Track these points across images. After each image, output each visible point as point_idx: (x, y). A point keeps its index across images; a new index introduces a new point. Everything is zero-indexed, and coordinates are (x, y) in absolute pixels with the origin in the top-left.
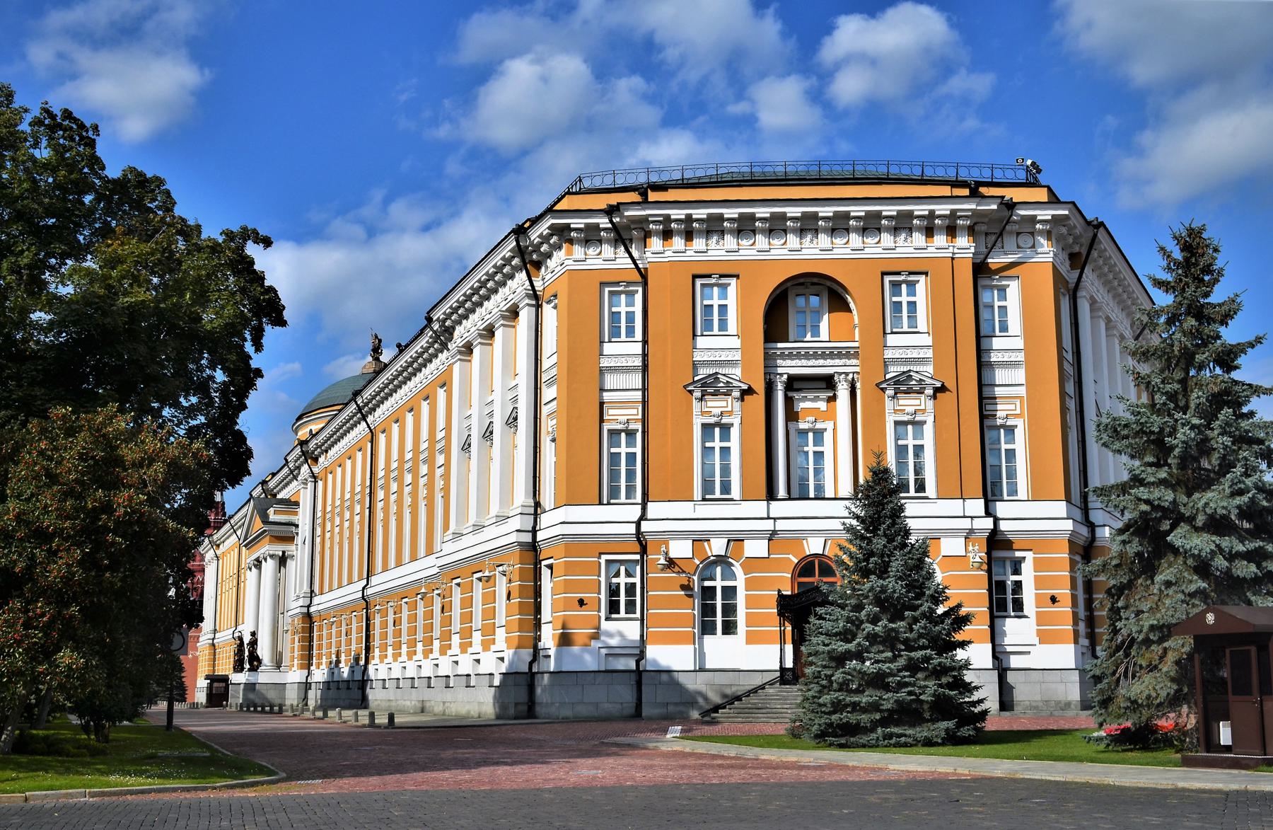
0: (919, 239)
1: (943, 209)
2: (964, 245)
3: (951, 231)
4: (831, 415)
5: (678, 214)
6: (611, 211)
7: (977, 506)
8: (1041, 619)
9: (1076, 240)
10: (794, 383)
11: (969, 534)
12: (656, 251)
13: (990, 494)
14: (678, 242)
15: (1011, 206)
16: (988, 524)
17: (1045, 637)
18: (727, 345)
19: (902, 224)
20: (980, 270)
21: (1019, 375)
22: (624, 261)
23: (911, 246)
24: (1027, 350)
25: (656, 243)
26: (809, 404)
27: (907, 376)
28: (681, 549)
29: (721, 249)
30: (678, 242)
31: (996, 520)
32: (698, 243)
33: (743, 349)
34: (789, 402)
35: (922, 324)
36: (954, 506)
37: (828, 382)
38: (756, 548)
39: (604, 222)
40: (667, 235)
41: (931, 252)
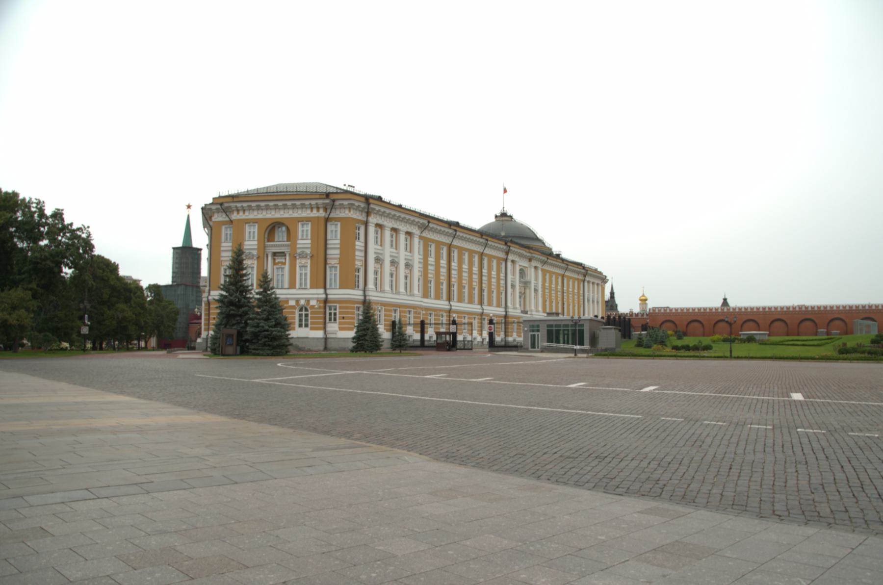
0: (309, 211)
1: (313, 202)
2: (322, 213)
3: (318, 209)
4: (284, 264)
5: (239, 205)
6: (221, 204)
7: (322, 291)
8: (340, 323)
9: (364, 208)
10: (274, 254)
11: (318, 300)
12: (235, 216)
13: (325, 288)
14: (241, 213)
15: (334, 201)
16: (324, 296)
17: (341, 329)
21: (338, 252)
22: (227, 219)
23: (307, 213)
24: (341, 244)
25: (235, 213)
27: (303, 252)
30: (241, 213)
31: (327, 295)
32: (247, 213)
33: (258, 245)
35: (309, 237)
37: (283, 254)
39: (219, 206)
40: (238, 211)
41: (312, 215)
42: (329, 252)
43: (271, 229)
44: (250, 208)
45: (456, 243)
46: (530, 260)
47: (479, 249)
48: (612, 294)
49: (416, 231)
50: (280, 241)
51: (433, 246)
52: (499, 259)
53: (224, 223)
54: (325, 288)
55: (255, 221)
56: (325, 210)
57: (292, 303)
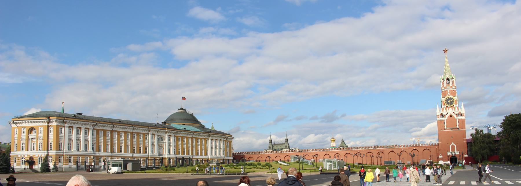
2: (46, 124)
7: (46, 151)
10: (32, 138)
12: (18, 125)
13: (48, 150)
18: (24, 136)
19: (40, 122)
20: (48, 127)
23: (41, 124)
26: (33, 140)
28: (19, 156)
29: (24, 125)
31: (48, 152)
34: (32, 141)
36: (44, 151)
38: (26, 156)
42: (50, 137)
43: (31, 130)
44: (23, 123)
45: (114, 129)
46: (166, 133)
47: (131, 131)
48: (287, 140)
49: (91, 128)
50: (33, 135)
51: (102, 132)
52: (144, 134)
53: (15, 128)
54: (48, 150)
55: (25, 127)
56: (48, 123)
57: (37, 156)
